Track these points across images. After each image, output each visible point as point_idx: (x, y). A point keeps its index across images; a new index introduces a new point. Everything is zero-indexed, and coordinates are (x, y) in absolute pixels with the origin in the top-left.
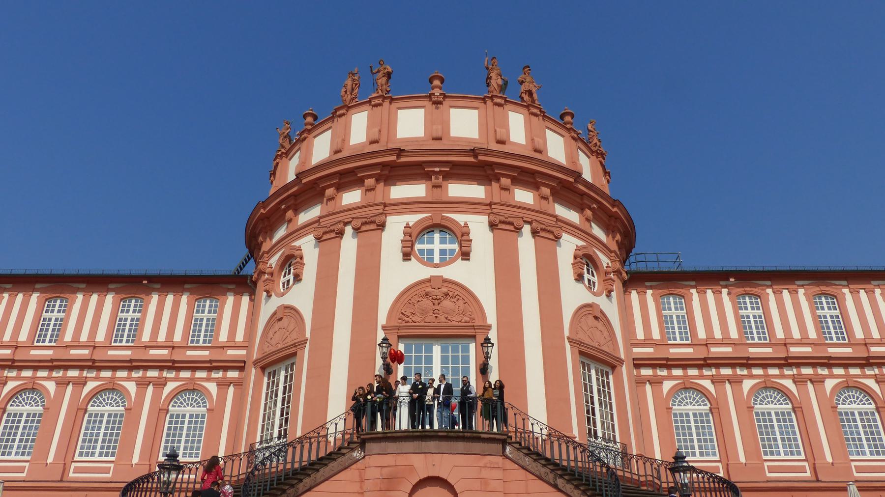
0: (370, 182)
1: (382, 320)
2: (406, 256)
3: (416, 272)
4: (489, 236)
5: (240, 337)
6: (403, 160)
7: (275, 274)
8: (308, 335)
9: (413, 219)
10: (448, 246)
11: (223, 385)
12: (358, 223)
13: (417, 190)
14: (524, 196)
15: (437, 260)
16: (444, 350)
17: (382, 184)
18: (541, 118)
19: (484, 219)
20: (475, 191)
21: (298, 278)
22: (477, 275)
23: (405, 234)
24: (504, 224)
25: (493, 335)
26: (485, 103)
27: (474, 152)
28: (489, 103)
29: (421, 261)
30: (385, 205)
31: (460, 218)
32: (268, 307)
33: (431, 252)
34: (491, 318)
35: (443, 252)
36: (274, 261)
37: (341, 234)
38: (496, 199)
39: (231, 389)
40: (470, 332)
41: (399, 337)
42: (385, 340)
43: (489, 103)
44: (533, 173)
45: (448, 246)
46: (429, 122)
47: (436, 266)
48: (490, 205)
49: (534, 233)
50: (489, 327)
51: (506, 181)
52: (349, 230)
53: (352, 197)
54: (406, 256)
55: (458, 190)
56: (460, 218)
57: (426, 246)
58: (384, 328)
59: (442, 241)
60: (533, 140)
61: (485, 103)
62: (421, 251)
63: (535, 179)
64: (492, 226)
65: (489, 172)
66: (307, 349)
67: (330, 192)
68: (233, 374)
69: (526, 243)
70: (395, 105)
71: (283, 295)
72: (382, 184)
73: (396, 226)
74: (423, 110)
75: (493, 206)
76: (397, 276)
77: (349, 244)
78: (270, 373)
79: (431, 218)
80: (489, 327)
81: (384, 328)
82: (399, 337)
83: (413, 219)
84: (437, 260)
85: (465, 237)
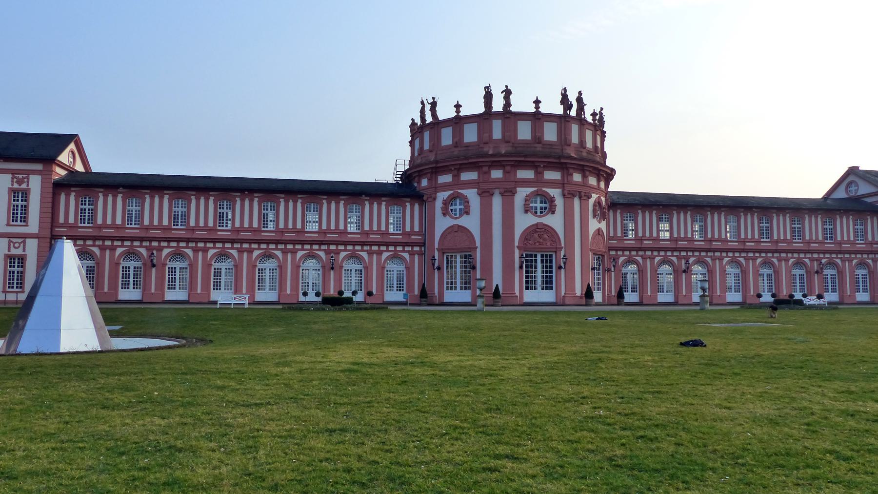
0: (508, 168)
1: (516, 244)
5: (417, 229)
10: (544, 205)
11: (412, 254)
12: (502, 191)
14: (577, 177)
15: (539, 213)
16: (542, 256)
19: (559, 191)
22: (556, 221)
24: (568, 196)
27: (559, 157)
34: (563, 245)
35: (541, 208)
36: (442, 196)
37: (492, 194)
39: (416, 257)
44: (583, 166)
45: (544, 205)
46: (534, 130)
47: (539, 217)
49: (580, 198)
52: (497, 192)
53: (497, 174)
54: (526, 212)
64: (564, 196)
67: (485, 169)
68: (416, 249)
69: (577, 202)
76: (523, 222)
77: (497, 202)
79: (537, 191)
84: (539, 213)
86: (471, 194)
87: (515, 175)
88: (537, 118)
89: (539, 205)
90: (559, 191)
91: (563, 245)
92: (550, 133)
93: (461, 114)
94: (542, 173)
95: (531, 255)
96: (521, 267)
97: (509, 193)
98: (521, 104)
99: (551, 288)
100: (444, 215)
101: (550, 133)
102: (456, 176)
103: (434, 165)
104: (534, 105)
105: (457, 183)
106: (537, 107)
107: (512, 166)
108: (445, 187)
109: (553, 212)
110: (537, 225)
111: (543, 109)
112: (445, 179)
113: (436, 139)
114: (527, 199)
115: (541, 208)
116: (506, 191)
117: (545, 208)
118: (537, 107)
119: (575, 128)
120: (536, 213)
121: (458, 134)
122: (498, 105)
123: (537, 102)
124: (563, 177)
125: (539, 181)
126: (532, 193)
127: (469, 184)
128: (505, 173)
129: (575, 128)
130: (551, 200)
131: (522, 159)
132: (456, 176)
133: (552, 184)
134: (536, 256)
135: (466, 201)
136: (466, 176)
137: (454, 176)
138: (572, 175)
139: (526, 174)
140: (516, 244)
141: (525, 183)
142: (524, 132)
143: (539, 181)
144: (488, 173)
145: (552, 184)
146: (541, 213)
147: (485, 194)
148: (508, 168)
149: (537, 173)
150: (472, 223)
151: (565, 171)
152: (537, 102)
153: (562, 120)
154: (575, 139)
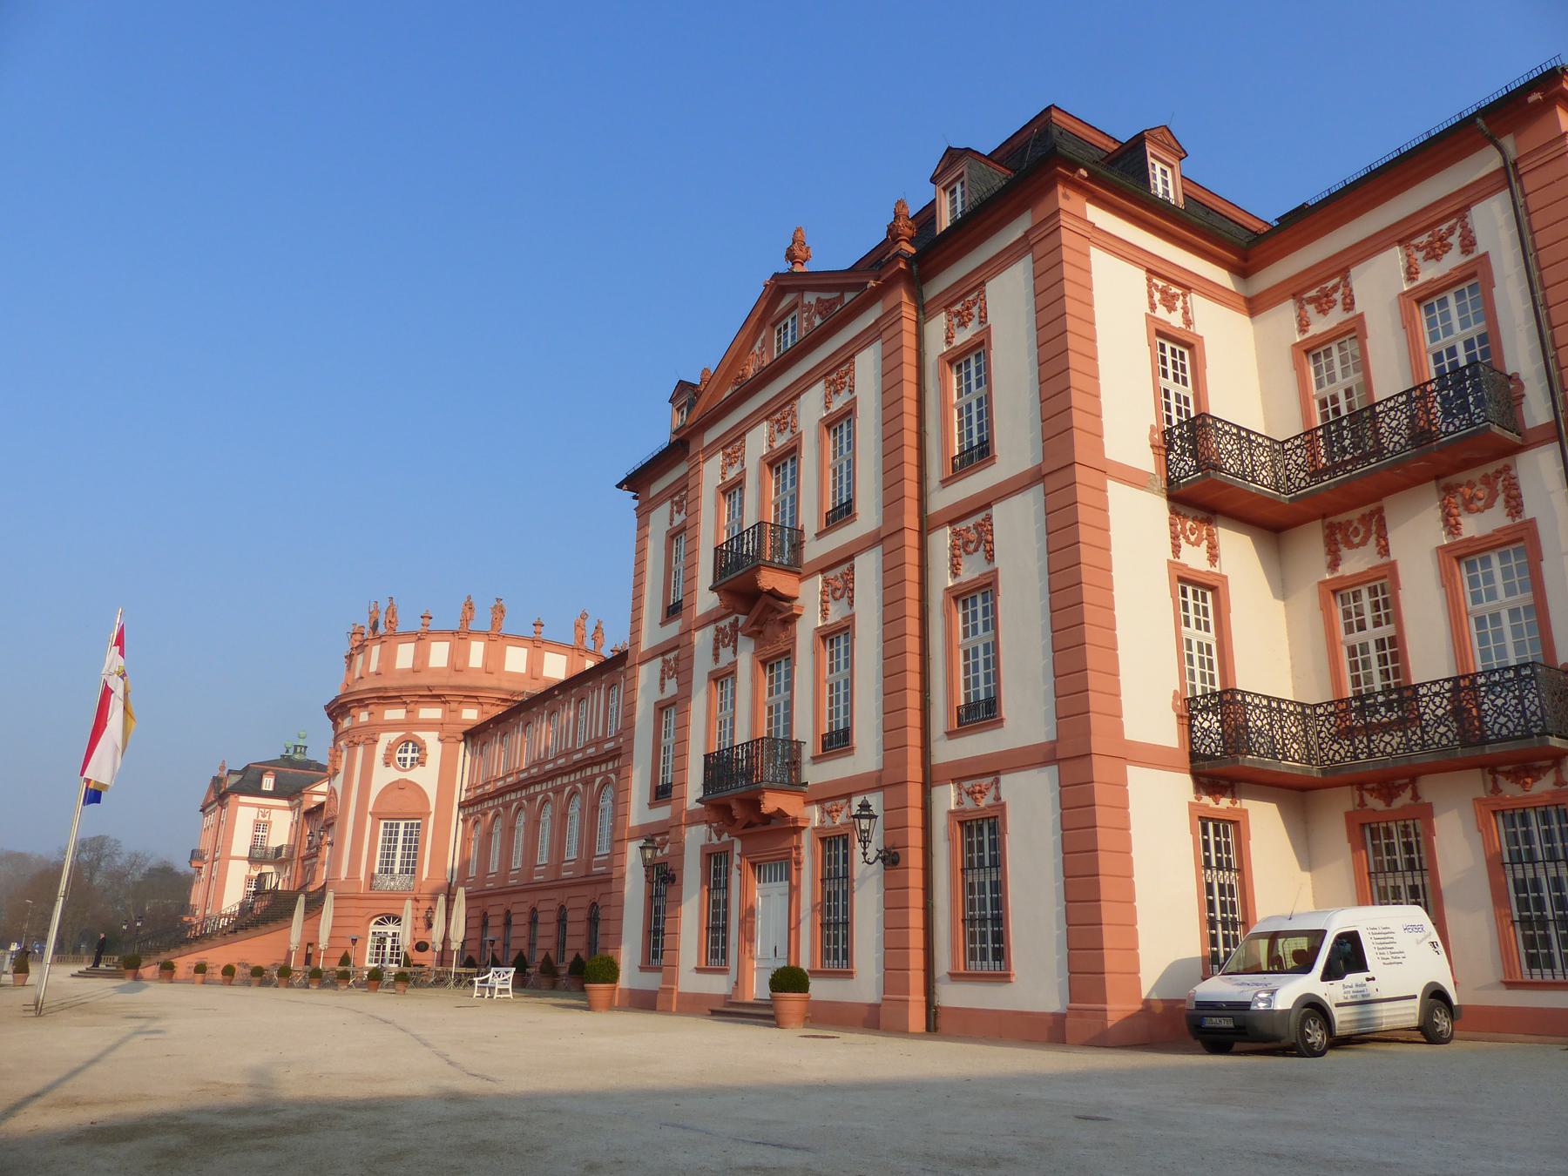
2: (387, 764)
3: (393, 774)
4: (439, 745)
9: (394, 736)
19: (436, 734)
22: (427, 777)
27: (429, 689)
29: (397, 768)
31: (422, 735)
34: (432, 808)
53: (364, 717)
54: (387, 764)
56: (422, 735)
64: (440, 740)
73: (386, 738)
76: (383, 776)
77: (360, 750)
83: (394, 736)
89: (409, 755)
90: (436, 734)
91: (432, 808)
109: (423, 764)
114: (391, 749)
124: (444, 714)
130: (420, 747)
133: (429, 725)
139: (396, 714)
142: (405, 655)
143: (412, 724)
145: (429, 725)
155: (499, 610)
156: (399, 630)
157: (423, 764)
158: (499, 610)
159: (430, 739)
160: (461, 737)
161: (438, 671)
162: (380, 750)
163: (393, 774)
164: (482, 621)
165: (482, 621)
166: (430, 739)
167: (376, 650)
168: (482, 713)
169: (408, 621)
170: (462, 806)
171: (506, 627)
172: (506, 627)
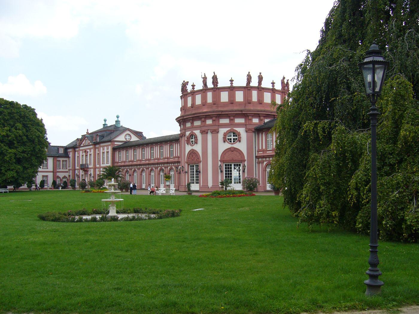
2: (224, 142)
3: (227, 146)
6: (223, 113)
7: (189, 138)
8: (201, 160)
10: (235, 137)
13: (226, 121)
15: (232, 142)
17: (217, 118)
18: (262, 90)
19: (244, 129)
20: (241, 121)
21: (196, 143)
22: (242, 146)
23: (224, 135)
25: (246, 163)
26: (245, 89)
27: (242, 111)
28: (246, 89)
30: (219, 125)
31: (238, 130)
32: (188, 148)
33: (231, 139)
34: (246, 158)
35: (234, 139)
36: (188, 133)
37: (207, 133)
38: (247, 124)
40: (241, 162)
41: (223, 163)
42: (220, 165)
43: (246, 89)
45: (235, 137)
47: (232, 144)
48: (246, 125)
50: (246, 160)
51: (250, 117)
52: (209, 131)
53: (209, 122)
54: (224, 142)
55: (238, 121)
56: (238, 130)
57: (229, 138)
58: (220, 161)
59: (234, 136)
60: (259, 99)
61: (245, 89)
62: (228, 139)
63: (259, 115)
64: (246, 132)
65: (246, 115)
66: (201, 163)
70: (220, 90)
71: (192, 146)
72: (217, 118)
73: (222, 131)
74: (228, 92)
75: (247, 125)
76: (223, 147)
78: (191, 166)
79: (230, 130)
80: (246, 160)
81: (220, 161)
82: (223, 163)
84: (232, 142)
85: (239, 136)
86: (197, 132)
87: (219, 121)
88: (232, 89)
89: (232, 137)
90: (244, 129)
92: (239, 97)
93: (195, 90)
94: (233, 120)
95: (228, 165)
96: (222, 172)
97: (215, 132)
98: (223, 83)
99: (240, 183)
100: (188, 144)
101: (239, 97)
102: (192, 123)
103: (182, 118)
104: (230, 82)
105: (193, 127)
106: (232, 84)
107: (216, 117)
108: (189, 129)
109: (240, 141)
110: (230, 148)
111: (235, 84)
112: (188, 125)
113: (186, 102)
114: (225, 135)
115: (234, 139)
116: (213, 131)
117: (236, 139)
118: (232, 84)
119: (255, 94)
120: (231, 142)
121: (194, 100)
122: (210, 85)
123: (232, 81)
124: (245, 120)
125: (232, 124)
126: (227, 131)
127: (197, 128)
128: (213, 121)
129: (255, 94)
130: (239, 134)
131: (220, 113)
132: (192, 123)
134: (231, 165)
135: (196, 137)
136: (197, 123)
137: (191, 123)
138: (251, 120)
140: (219, 159)
141: (224, 126)
142: (224, 97)
143: (232, 124)
144: (205, 121)
145: (239, 125)
146: (234, 141)
147: (204, 133)
148: (214, 118)
149: (231, 120)
150: (198, 148)
151: (247, 118)
152: (232, 81)
153: (247, 89)
154: (255, 98)
155: (260, 78)
156: (219, 85)
157: (240, 141)
158: (260, 78)
159: (241, 131)
160: (253, 130)
161: (240, 103)
162: (221, 136)
163: (227, 146)
164: (254, 83)
165: (254, 83)
166: (241, 131)
167: (210, 95)
168: (260, 120)
169: (223, 83)
170: (256, 157)
171: (263, 85)
172: (263, 85)
